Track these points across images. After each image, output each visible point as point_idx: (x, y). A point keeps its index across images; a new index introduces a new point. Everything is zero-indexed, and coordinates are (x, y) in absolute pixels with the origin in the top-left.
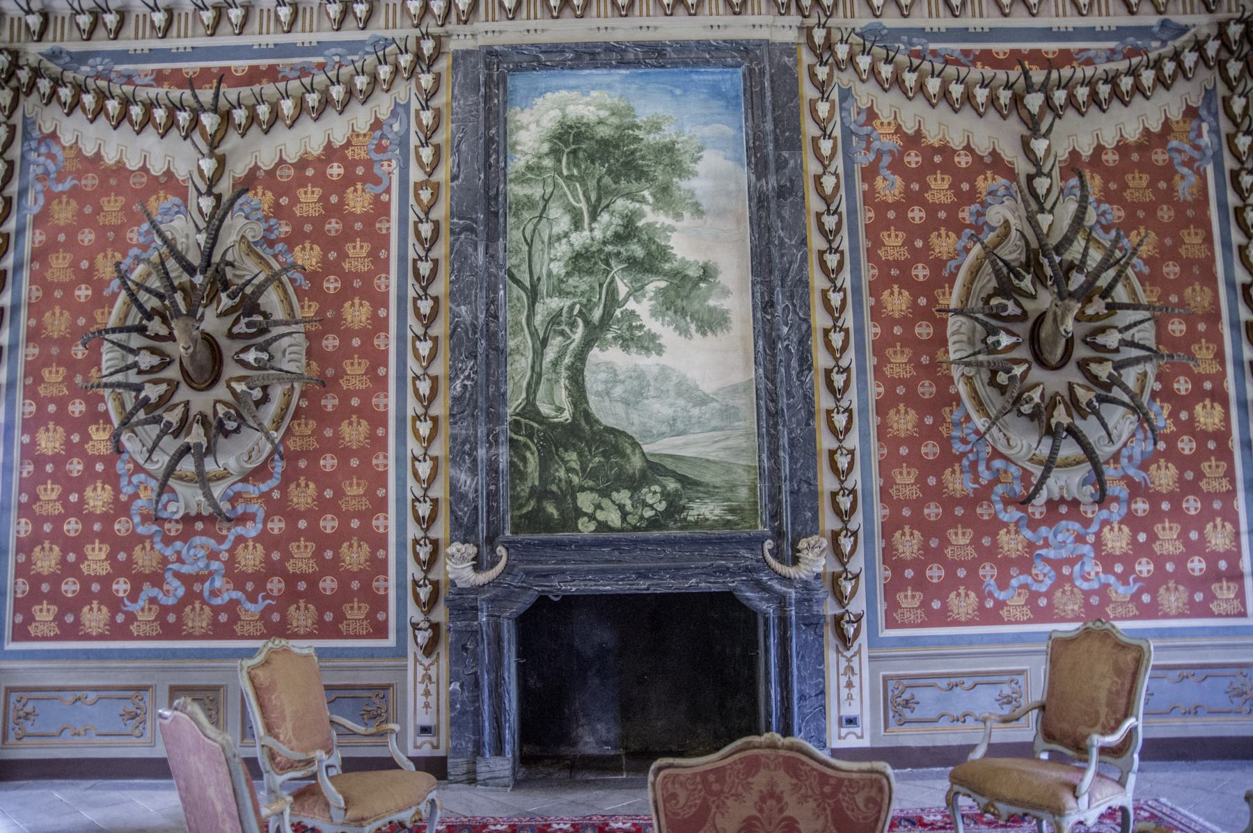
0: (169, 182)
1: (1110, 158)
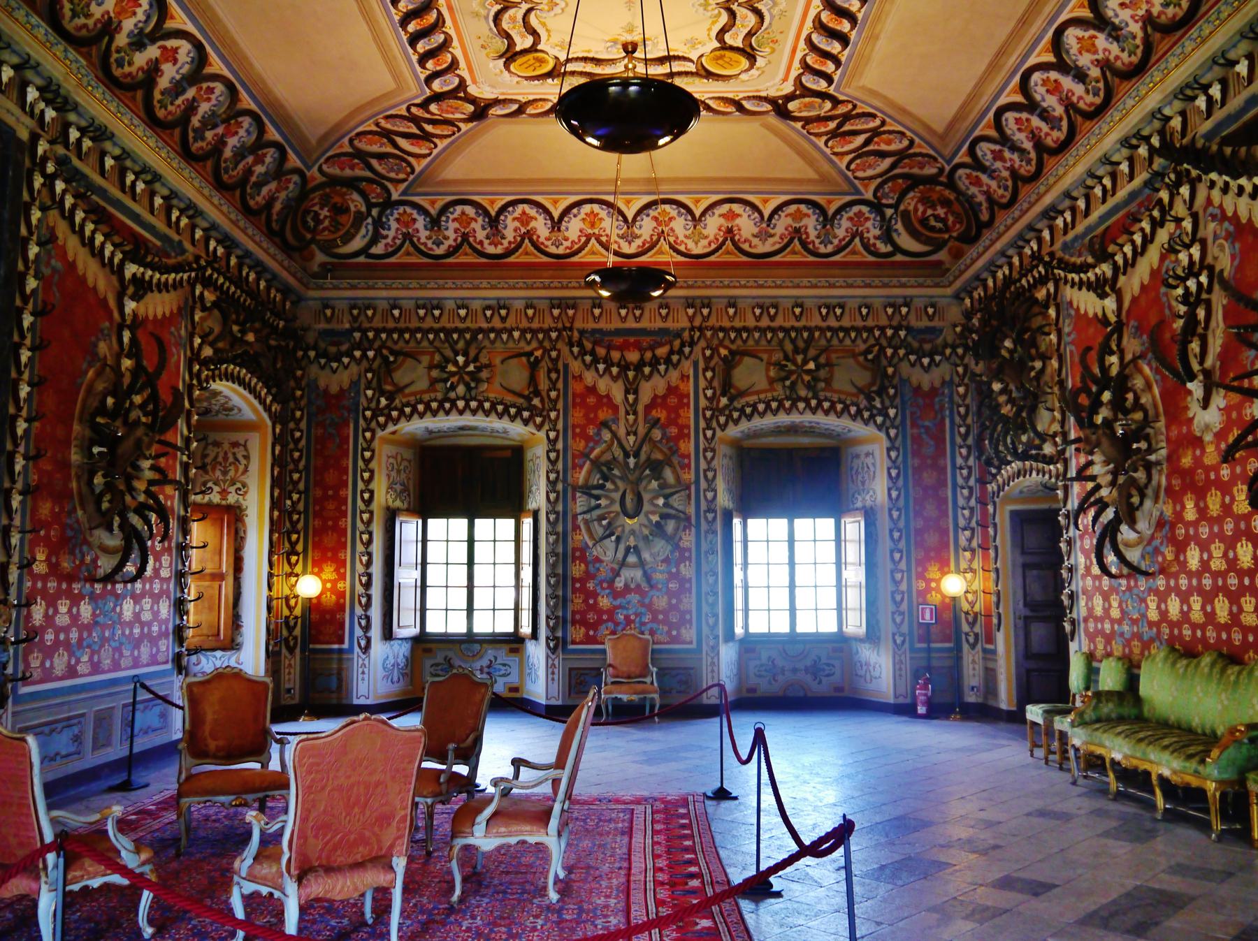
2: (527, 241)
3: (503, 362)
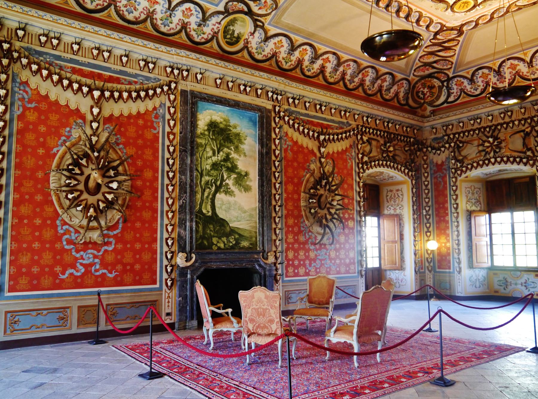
0: (77, 113)
1: (336, 155)
2: (517, 77)
3: (510, 137)
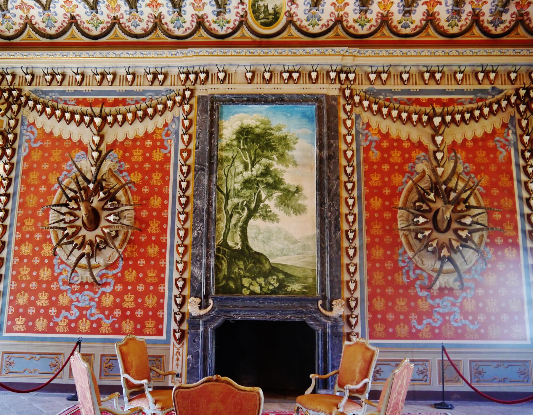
0: (81, 146)
1: (470, 144)
